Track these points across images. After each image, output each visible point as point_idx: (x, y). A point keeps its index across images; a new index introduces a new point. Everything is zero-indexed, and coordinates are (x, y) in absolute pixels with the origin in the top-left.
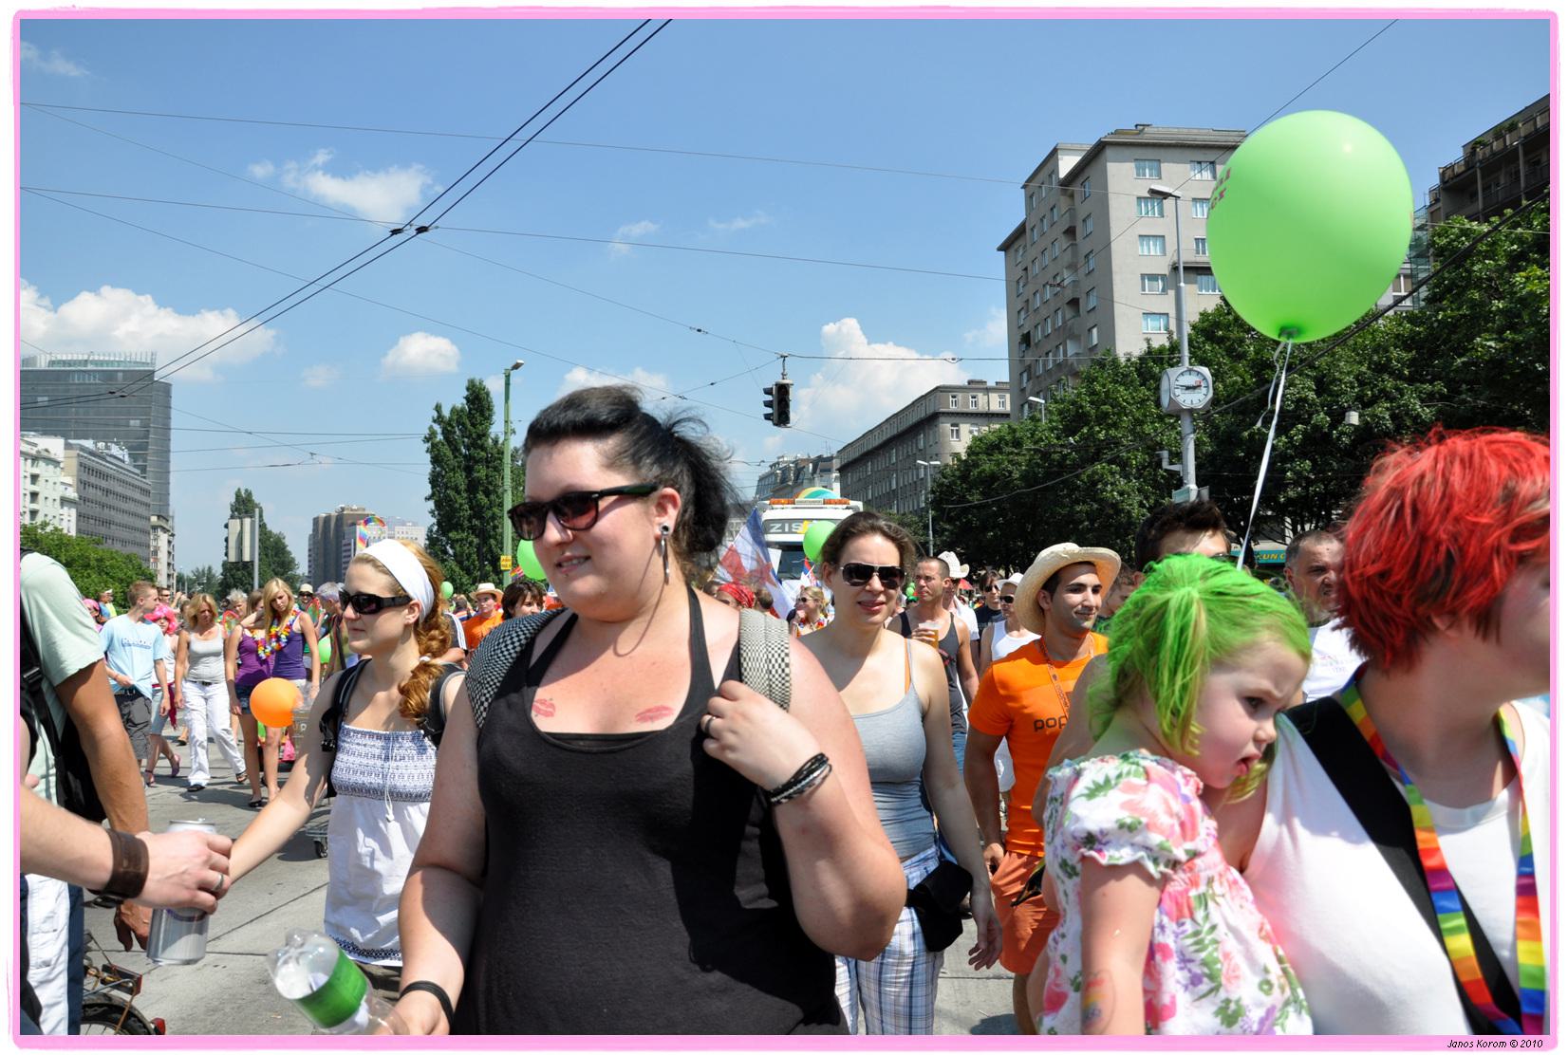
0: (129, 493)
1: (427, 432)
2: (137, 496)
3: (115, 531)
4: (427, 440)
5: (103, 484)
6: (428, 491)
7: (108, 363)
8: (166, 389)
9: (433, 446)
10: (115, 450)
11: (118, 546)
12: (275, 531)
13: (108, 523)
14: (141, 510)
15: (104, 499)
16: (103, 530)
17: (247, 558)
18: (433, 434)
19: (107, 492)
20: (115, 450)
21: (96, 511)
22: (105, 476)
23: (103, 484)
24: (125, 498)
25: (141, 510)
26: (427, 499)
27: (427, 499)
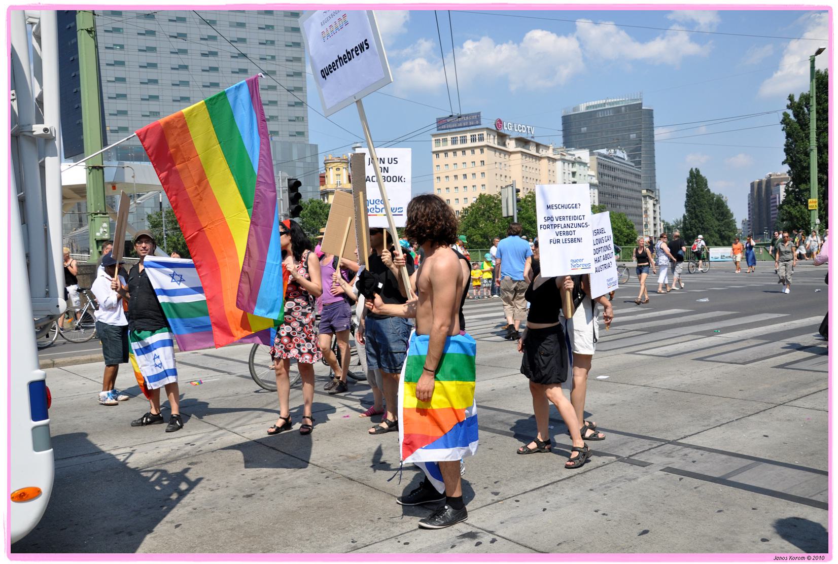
0: (628, 177)
1: (781, 117)
2: (633, 178)
3: (621, 200)
4: (783, 122)
5: (612, 173)
6: (784, 157)
7: (613, 103)
8: (650, 113)
9: (787, 124)
10: (619, 153)
11: (623, 209)
12: (717, 193)
13: (616, 196)
14: (636, 187)
15: (614, 183)
16: (614, 200)
17: (511, 214)
18: (786, 115)
19: (615, 178)
20: (619, 153)
21: (609, 189)
22: (613, 169)
23: (612, 173)
24: (626, 180)
25: (636, 187)
26: (784, 163)
27: (784, 163)
